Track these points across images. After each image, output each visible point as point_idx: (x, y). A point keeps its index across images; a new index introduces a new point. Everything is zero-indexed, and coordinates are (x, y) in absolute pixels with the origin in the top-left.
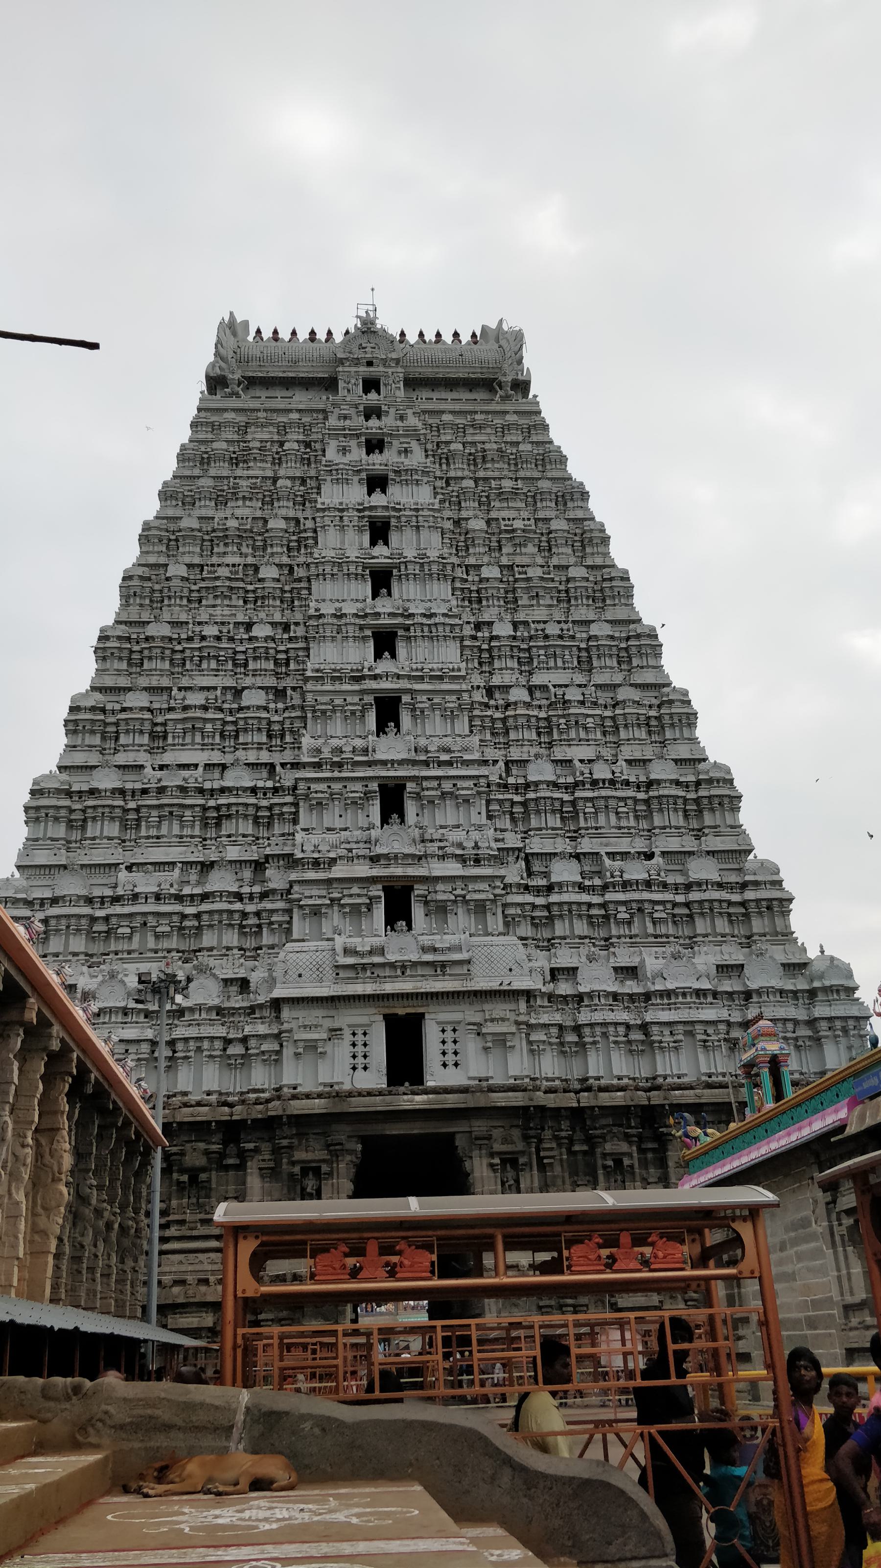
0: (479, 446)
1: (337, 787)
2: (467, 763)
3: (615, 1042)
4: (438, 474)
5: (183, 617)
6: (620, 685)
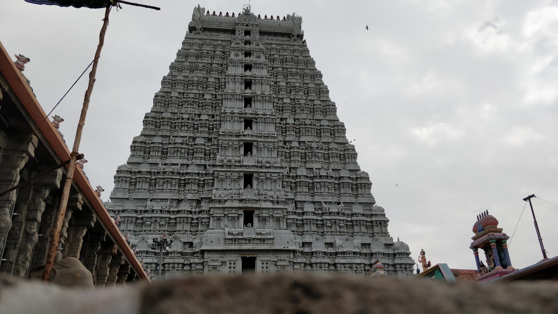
0: (285, 57)
1: (228, 174)
2: (276, 168)
3: (324, 270)
4: (270, 65)
5: (176, 111)
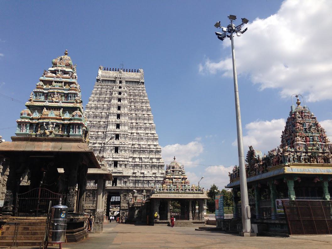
2: (127, 145)
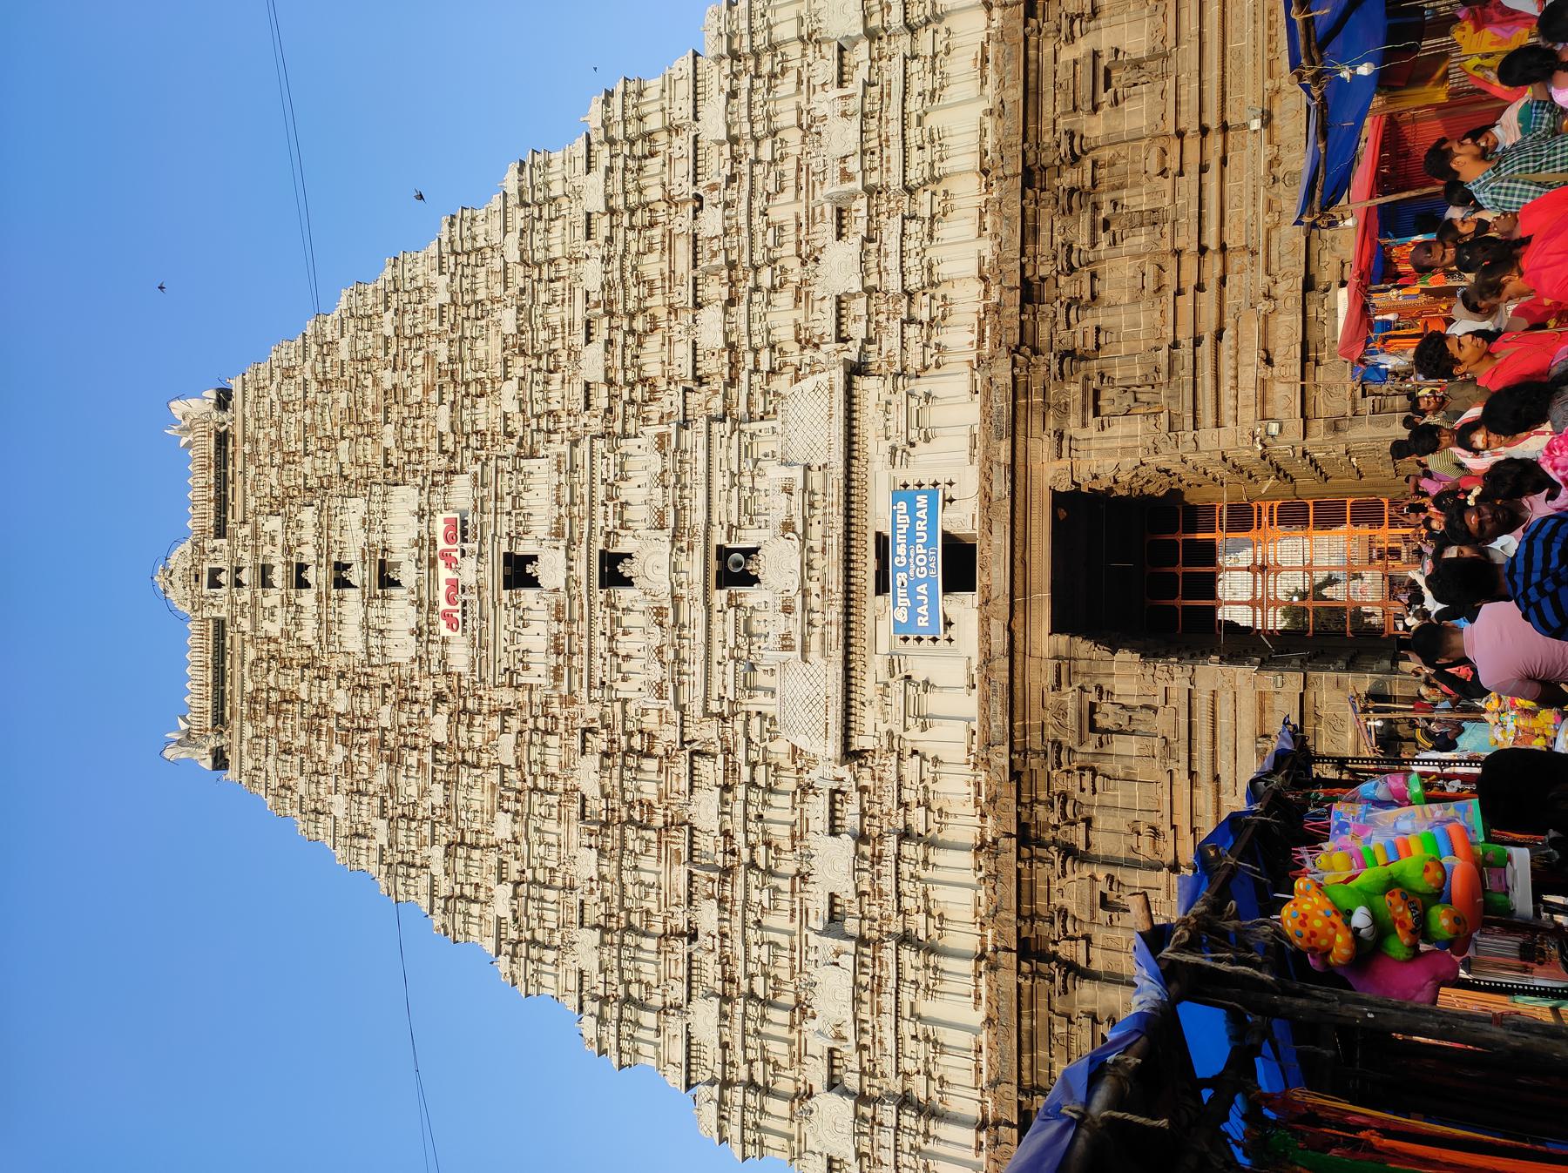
6: (506, 263)
